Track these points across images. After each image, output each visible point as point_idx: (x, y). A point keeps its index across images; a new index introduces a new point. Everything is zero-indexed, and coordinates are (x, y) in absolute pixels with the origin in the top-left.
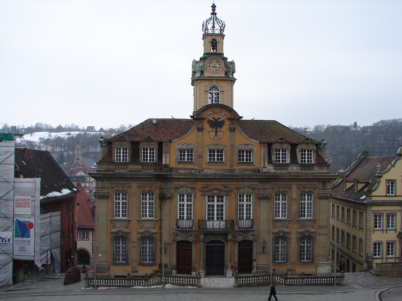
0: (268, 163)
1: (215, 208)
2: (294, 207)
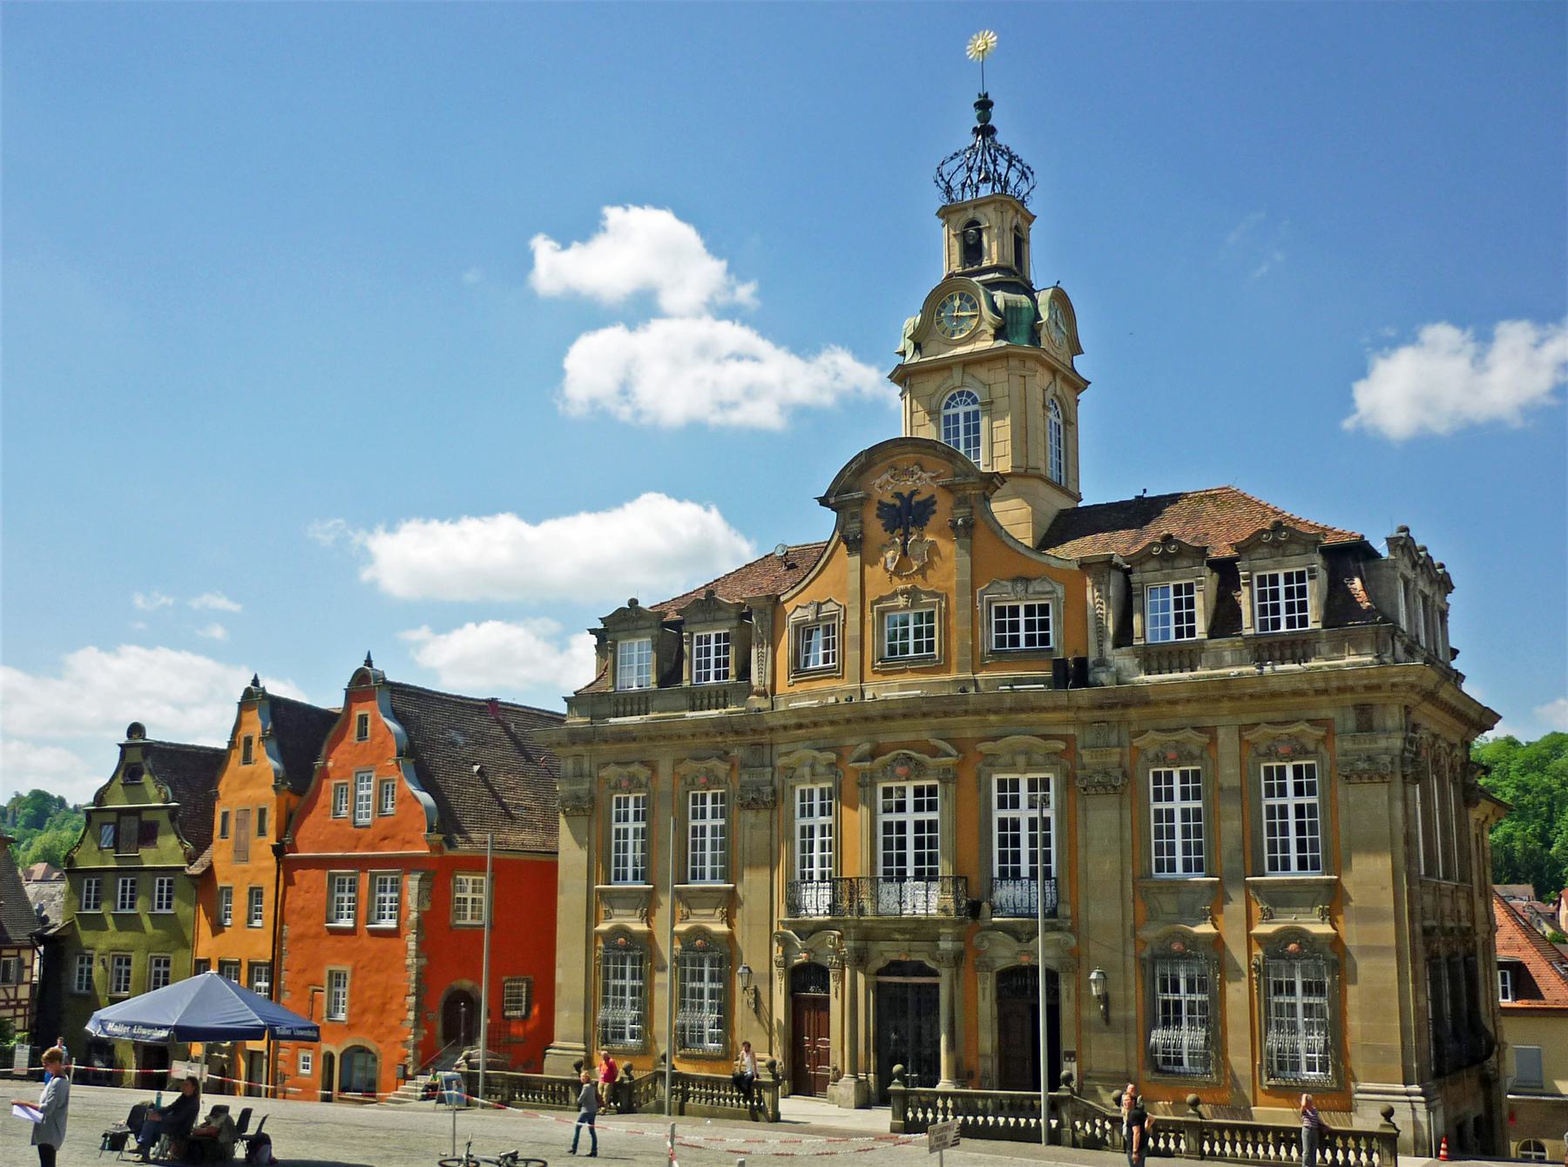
0: (1117, 645)
1: (910, 836)
2: (1231, 826)
